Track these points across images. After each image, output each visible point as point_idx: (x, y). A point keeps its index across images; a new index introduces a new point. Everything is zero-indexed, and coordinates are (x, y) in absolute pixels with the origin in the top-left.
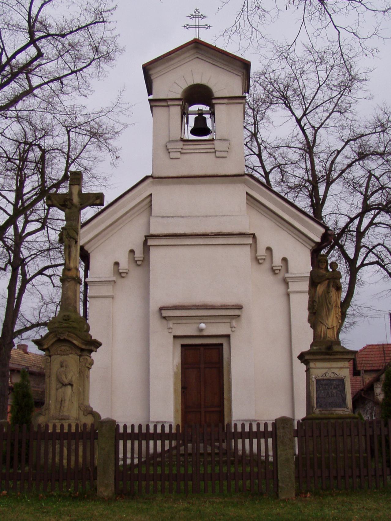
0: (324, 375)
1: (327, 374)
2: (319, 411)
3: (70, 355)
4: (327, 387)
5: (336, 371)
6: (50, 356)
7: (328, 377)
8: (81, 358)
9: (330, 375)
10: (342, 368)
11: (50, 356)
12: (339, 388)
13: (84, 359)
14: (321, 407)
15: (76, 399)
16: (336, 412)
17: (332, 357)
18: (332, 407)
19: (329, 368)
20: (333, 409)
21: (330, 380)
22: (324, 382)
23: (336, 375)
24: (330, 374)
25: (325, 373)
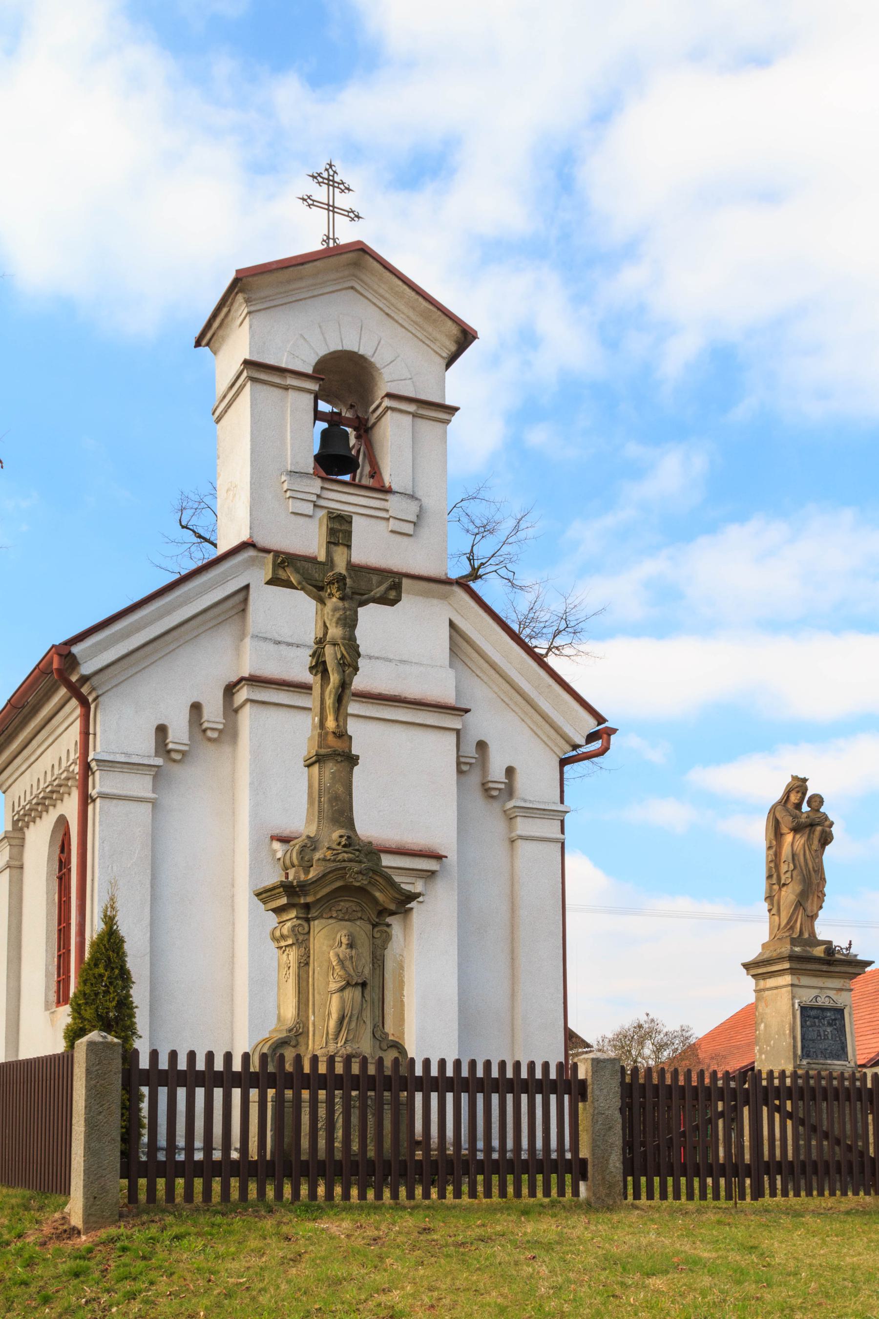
0: (814, 1000)
1: (819, 999)
2: (808, 1063)
3: (358, 923)
4: (817, 1020)
5: (831, 993)
6: (308, 920)
7: (820, 1004)
8: (376, 930)
9: (823, 1001)
10: (841, 990)
11: (308, 920)
12: (835, 1025)
13: (381, 932)
14: (808, 1056)
15: (369, 1015)
16: (833, 1067)
17: (832, 969)
18: (826, 1058)
19: (821, 988)
20: (829, 1062)
21: (823, 1009)
22: (813, 1013)
23: (832, 1002)
24: (823, 997)
25: (816, 997)
